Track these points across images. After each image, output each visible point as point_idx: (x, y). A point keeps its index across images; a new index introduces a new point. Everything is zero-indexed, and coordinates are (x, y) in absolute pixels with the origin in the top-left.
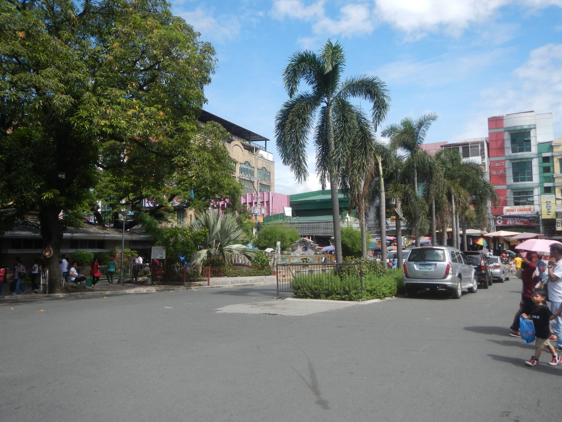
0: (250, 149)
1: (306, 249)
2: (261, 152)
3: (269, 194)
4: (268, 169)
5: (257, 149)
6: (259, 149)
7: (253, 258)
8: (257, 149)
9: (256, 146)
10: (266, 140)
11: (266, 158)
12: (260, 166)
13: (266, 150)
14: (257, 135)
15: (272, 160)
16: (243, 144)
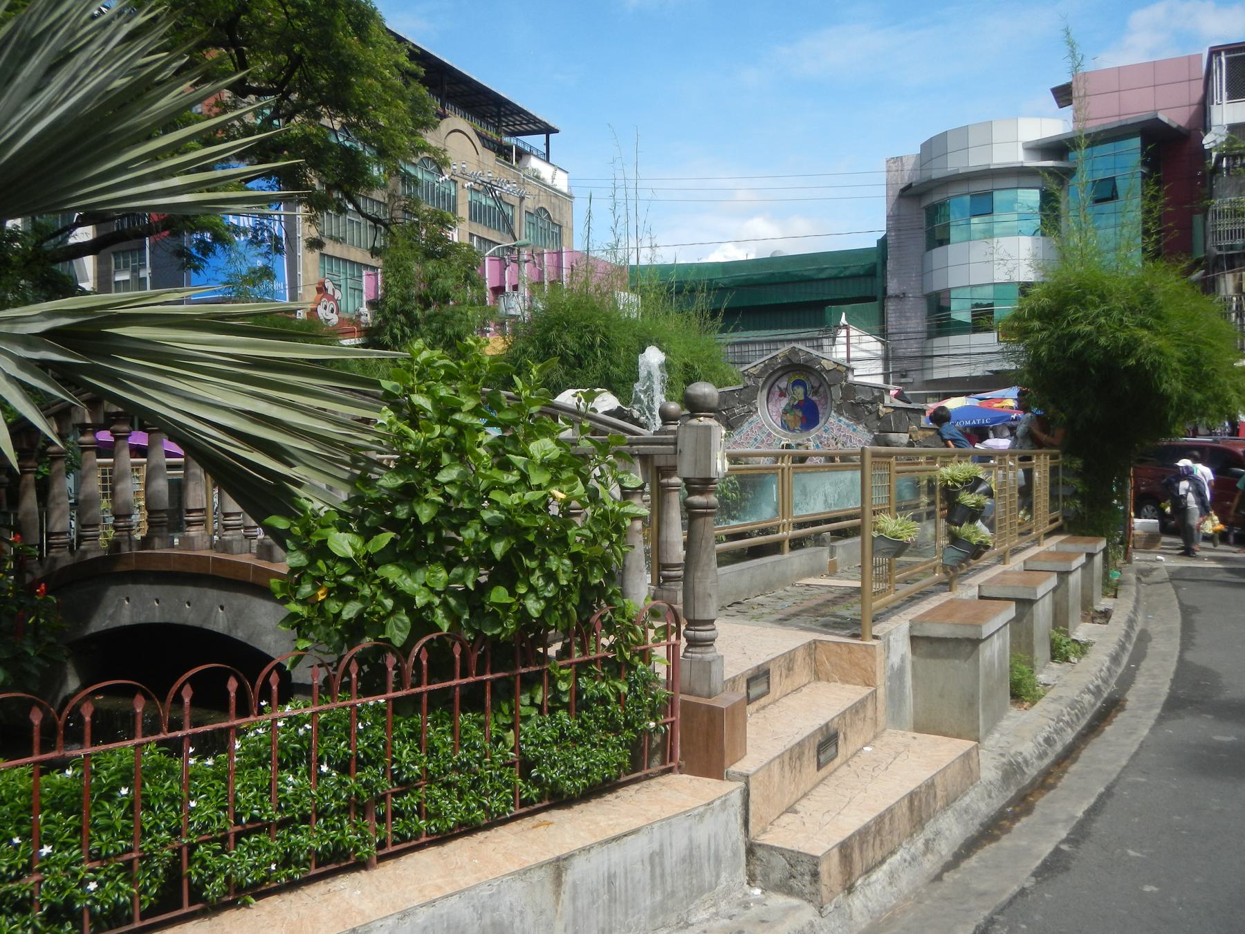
0: (503, 152)
1: (808, 415)
2: (534, 163)
3: (559, 253)
4: (556, 216)
5: (521, 154)
6: (529, 154)
7: (320, 493)
8: (521, 154)
9: (521, 145)
10: (548, 130)
11: (549, 182)
12: (529, 204)
13: (548, 161)
14: (519, 111)
15: (565, 190)
16: (478, 135)
